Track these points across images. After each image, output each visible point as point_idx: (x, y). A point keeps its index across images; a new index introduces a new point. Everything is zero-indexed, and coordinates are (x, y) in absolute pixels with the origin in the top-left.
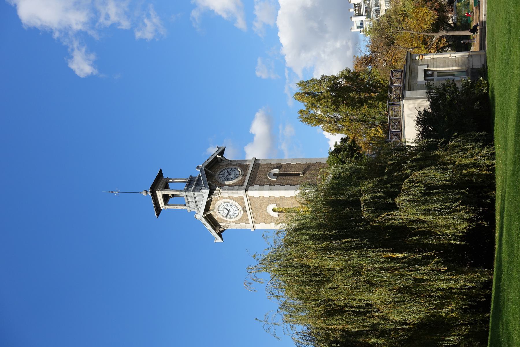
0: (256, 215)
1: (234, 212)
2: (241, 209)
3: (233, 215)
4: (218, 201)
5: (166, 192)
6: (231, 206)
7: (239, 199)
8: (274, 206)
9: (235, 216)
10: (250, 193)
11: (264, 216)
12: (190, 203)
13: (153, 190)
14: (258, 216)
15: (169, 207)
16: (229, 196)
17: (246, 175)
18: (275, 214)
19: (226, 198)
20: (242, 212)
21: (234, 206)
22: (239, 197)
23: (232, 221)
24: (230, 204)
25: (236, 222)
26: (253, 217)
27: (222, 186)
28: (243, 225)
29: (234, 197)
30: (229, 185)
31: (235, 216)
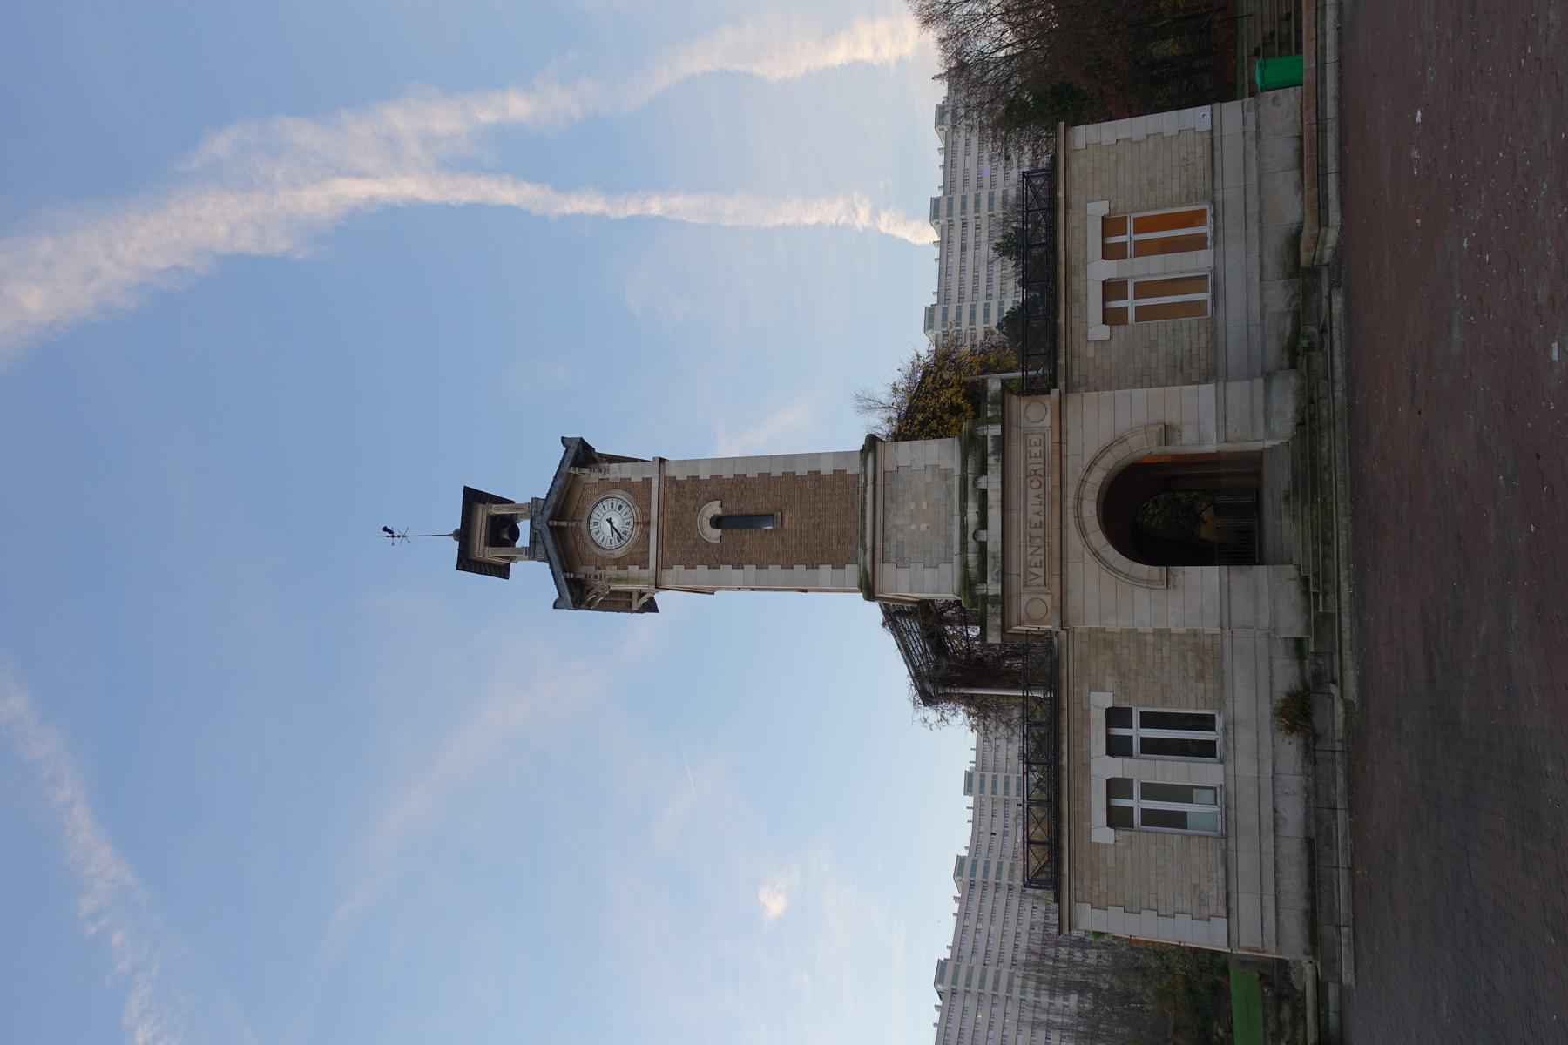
17: (647, 524)
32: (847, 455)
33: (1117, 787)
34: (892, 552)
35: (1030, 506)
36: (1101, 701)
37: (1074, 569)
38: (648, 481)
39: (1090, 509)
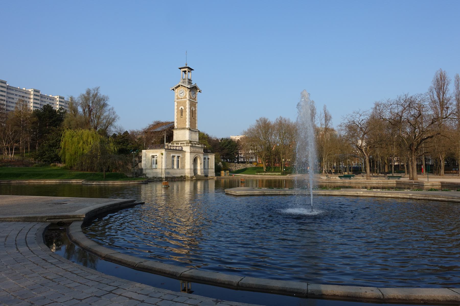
5: (187, 71)
8: (183, 108)
10: (188, 102)
13: (189, 68)
15: (182, 72)
18: (180, 109)
20: (181, 97)
25: (177, 96)
27: (190, 91)
28: (176, 97)
30: (190, 94)
32: (197, 128)
33: (174, 156)
34: (192, 132)
35: (197, 150)
36: (180, 155)
37: (193, 153)
38: (196, 100)
39: (197, 156)
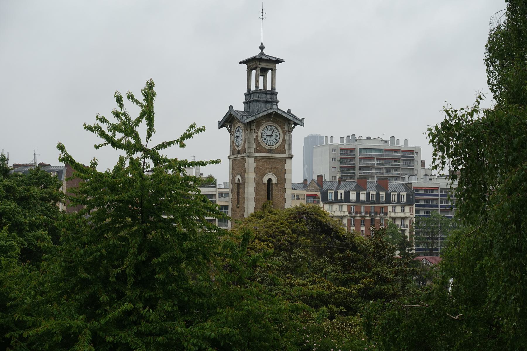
0: (264, 161)
1: (269, 141)
2: (273, 148)
3: (265, 139)
4: (281, 128)
6: (276, 139)
7: (283, 149)
8: (274, 181)
9: (264, 141)
11: (263, 169)
12: (265, 95)
14: (264, 163)
16: (286, 140)
18: (265, 180)
19: (284, 137)
20: (268, 148)
21: (275, 143)
22: (285, 150)
23: (257, 136)
24: (278, 139)
26: (263, 158)
29: (285, 145)
31: (264, 141)
